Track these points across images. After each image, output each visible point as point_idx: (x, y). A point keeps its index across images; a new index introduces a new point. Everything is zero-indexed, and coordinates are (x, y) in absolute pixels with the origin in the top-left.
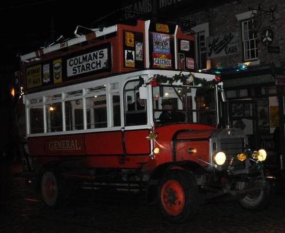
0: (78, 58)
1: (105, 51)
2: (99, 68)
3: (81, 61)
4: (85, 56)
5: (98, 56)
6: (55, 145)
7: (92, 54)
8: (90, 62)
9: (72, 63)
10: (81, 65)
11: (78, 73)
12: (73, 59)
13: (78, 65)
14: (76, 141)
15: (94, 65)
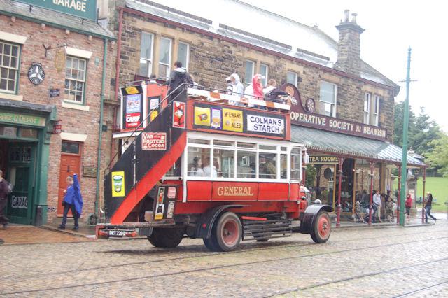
0: (259, 117)
1: (282, 121)
2: (277, 133)
3: (263, 121)
4: (266, 118)
5: (278, 123)
6: (226, 190)
7: (272, 119)
8: (270, 125)
9: (253, 119)
10: (263, 125)
11: (258, 130)
12: (255, 117)
13: (259, 123)
14: (249, 188)
15: (274, 129)
